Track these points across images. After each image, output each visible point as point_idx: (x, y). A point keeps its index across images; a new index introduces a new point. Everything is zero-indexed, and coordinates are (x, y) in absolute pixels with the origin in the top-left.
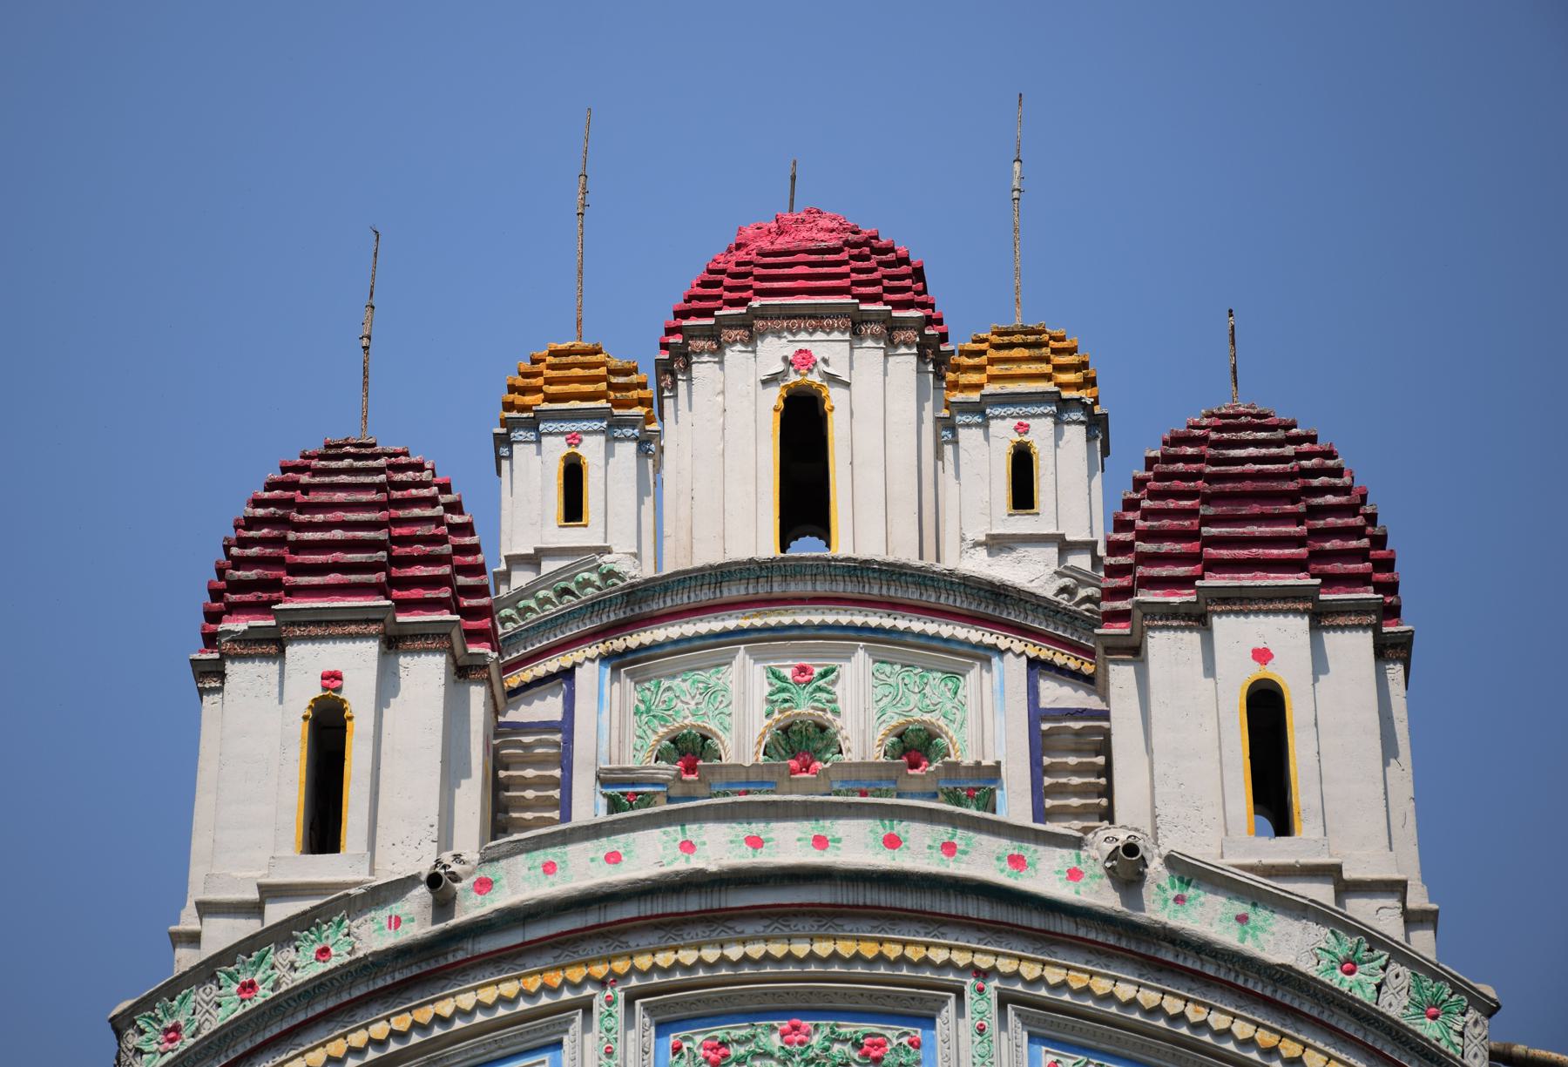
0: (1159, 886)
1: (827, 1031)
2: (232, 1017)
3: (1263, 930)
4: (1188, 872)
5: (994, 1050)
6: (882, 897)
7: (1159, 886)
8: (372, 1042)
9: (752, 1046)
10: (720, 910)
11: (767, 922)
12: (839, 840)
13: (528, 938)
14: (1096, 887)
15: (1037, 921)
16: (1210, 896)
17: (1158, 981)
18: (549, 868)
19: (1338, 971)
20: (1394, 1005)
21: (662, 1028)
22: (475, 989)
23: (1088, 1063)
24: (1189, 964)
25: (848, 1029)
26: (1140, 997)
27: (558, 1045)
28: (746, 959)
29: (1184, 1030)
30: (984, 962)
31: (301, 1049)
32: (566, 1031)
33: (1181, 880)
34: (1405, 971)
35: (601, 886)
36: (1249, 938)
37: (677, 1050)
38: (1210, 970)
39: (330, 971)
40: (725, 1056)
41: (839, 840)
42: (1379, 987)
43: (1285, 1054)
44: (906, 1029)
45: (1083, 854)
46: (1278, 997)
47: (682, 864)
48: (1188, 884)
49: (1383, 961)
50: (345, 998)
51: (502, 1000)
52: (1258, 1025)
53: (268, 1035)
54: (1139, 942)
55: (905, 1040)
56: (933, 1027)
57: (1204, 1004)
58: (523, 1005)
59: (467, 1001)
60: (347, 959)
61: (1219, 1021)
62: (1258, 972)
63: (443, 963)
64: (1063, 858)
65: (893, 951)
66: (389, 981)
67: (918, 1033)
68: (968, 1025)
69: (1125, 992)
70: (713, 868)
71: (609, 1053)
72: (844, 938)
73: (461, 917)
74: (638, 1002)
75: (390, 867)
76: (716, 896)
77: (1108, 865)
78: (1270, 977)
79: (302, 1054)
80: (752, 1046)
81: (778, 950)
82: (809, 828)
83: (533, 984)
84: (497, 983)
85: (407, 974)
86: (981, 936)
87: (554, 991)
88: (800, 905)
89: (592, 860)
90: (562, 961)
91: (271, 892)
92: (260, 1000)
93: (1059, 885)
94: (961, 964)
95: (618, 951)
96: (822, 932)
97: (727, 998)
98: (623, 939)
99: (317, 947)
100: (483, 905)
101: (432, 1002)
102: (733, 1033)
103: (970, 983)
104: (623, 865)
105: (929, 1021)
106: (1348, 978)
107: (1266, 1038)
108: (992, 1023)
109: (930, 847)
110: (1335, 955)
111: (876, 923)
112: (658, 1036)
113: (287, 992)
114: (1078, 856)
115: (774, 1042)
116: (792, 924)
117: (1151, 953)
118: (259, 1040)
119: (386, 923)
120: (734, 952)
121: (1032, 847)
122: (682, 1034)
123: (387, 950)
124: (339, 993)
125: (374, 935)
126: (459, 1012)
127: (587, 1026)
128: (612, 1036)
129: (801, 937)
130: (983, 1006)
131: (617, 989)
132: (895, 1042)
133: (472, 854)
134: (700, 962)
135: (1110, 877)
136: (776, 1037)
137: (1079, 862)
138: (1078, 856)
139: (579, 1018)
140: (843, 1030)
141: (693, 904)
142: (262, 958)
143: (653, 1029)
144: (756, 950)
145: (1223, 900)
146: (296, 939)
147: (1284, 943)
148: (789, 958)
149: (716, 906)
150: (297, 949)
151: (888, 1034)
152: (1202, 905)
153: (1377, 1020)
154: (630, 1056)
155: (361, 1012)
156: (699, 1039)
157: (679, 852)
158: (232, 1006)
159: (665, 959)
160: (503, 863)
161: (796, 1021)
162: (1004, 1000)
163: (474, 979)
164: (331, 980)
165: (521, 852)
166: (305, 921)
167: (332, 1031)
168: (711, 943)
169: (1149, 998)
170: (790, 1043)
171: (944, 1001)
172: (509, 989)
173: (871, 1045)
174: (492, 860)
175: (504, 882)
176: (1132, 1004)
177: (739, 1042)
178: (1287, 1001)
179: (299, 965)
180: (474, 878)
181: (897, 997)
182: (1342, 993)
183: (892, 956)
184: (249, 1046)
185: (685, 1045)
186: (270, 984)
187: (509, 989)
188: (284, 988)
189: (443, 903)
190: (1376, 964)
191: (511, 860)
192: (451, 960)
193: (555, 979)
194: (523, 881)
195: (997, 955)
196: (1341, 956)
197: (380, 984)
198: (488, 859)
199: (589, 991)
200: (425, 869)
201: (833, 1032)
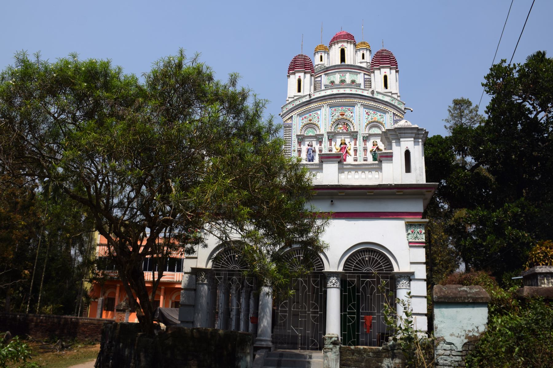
4: (378, 93)
20: (396, 104)
64: (367, 92)
82: (343, 89)
91: (295, 96)
125: (304, 100)
141: (333, 97)
147: (387, 99)
166: (298, 99)
179: (298, 103)
189: (310, 97)
194: (317, 95)
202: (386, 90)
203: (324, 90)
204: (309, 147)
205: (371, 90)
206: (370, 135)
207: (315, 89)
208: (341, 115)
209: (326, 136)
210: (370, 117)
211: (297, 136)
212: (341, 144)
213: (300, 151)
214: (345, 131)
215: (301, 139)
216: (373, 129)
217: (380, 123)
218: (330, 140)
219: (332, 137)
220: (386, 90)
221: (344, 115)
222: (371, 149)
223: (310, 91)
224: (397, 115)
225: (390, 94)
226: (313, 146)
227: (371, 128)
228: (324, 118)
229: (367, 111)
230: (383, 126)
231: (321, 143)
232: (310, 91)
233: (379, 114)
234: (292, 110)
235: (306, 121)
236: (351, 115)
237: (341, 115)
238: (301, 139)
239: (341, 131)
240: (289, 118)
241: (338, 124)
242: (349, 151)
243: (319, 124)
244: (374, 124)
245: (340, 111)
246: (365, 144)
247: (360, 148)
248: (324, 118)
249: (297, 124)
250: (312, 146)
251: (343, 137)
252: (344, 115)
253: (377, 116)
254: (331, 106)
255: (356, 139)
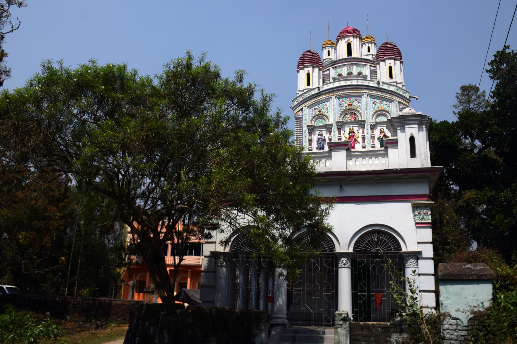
4: (384, 83)
20: (401, 93)
47: (339, 85)
64: (373, 82)
82: (350, 81)
91: (304, 89)
125: (313, 92)
147: (392, 88)
179: (307, 95)
189: (319, 89)
194: (326, 87)
202: (392, 81)
203: (332, 83)
204: (319, 137)
205: (376, 81)
206: (378, 123)
207: (324, 82)
208: (349, 105)
209: (335, 126)
210: (377, 106)
211: (308, 126)
212: (350, 133)
213: (310, 141)
214: (353, 120)
215: (311, 129)
216: (380, 117)
217: (386, 111)
218: (339, 129)
219: (340, 126)
220: (392, 81)
221: (351, 105)
222: (378, 136)
223: (319, 84)
224: (402, 103)
225: (395, 84)
226: (323, 135)
227: (378, 116)
228: (333, 110)
229: (373, 100)
230: (390, 114)
231: (330, 132)
232: (319, 84)
233: (385, 103)
234: (302, 103)
235: (315, 112)
236: (359, 105)
237: (349, 105)
238: (311, 129)
239: (349, 121)
240: (299, 110)
241: (346, 114)
242: (357, 139)
243: (328, 114)
244: (380, 113)
245: (347, 102)
246: (373, 132)
247: (368, 136)
248: (333, 110)
249: (308, 115)
250: (322, 135)
251: (351, 126)
252: (351, 105)
253: (384, 105)
254: (339, 97)
255: (364, 127)
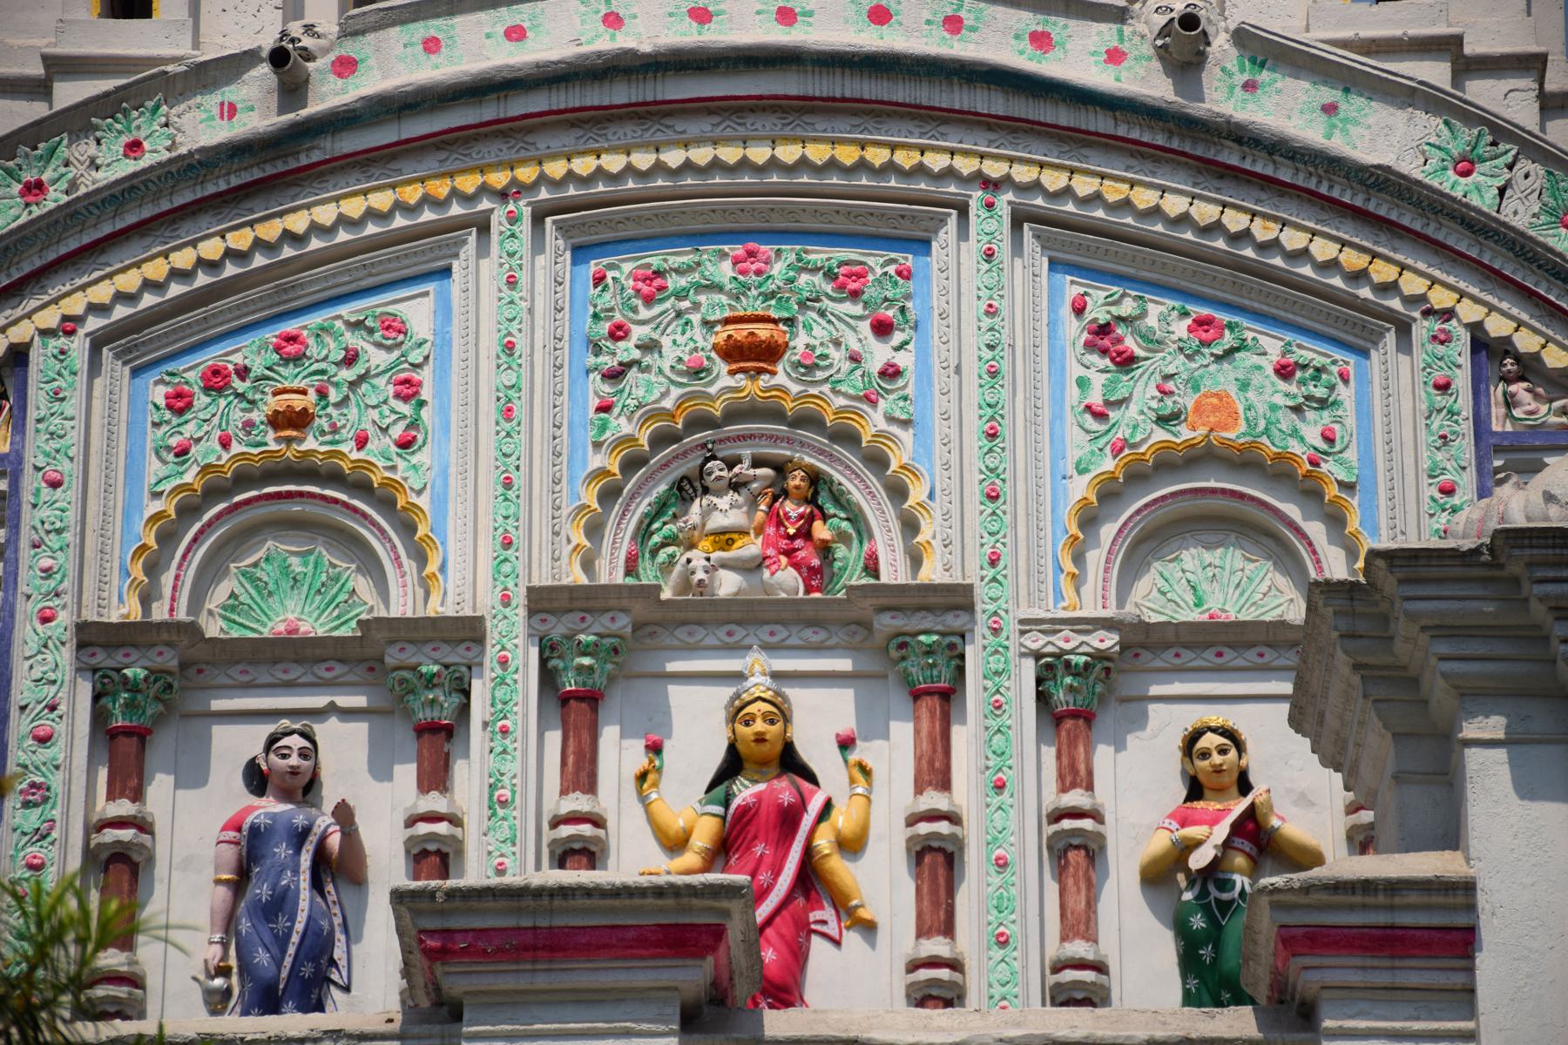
0: (1223, 70)
1: (792, 257)
2: (14, 225)
3: (1356, 122)
4: (1264, 51)
5: (1004, 280)
6: (866, 87)
7: (1223, 70)
8: (201, 263)
9: (696, 277)
10: (656, 103)
11: (716, 119)
12: (810, 14)
13: (404, 136)
14: (1142, 72)
15: (1063, 116)
16: (1289, 80)
17: (1218, 190)
18: (432, 45)
19: (1450, 172)
20: (1521, 214)
21: (580, 253)
22: (337, 199)
23: (1124, 295)
24: (1258, 169)
25: (819, 255)
26: (1193, 211)
27: (446, 272)
28: (688, 166)
29: (1249, 252)
30: (995, 169)
31: (108, 270)
32: (457, 256)
33: (1253, 61)
34: (1537, 169)
35: (500, 69)
36: (1337, 132)
37: (599, 280)
38: (1285, 175)
39: (144, 171)
40: (662, 288)
41: (810, 14)
42: (1502, 191)
43: (1376, 278)
44: (893, 255)
45: (1127, 30)
46: (1371, 207)
48: (1262, 65)
49: (1509, 158)
50: (165, 206)
51: (372, 214)
52: (1344, 243)
53: (63, 250)
54: (1195, 140)
55: (891, 269)
56: (928, 253)
57: (1275, 219)
58: (399, 222)
59: (326, 214)
60: (166, 156)
61: (1293, 240)
62: (1347, 177)
63: (293, 165)
64: (1101, 34)
65: (878, 156)
66: (223, 186)
67: (909, 260)
68: (972, 249)
69: (1175, 205)
70: (646, 48)
71: (512, 282)
72: (815, 140)
73: (314, 107)
74: (549, 220)
75: (220, 40)
76: (650, 85)
77: (1159, 43)
78: (1362, 182)
79: (110, 276)
80: (696, 277)
81: (730, 154)
83: (412, 194)
84: (365, 193)
85: (246, 177)
86: (992, 136)
87: (439, 204)
88: (760, 97)
89: (488, 36)
90: (448, 167)
91: (62, 66)
92: (51, 205)
93: (1094, 70)
94: (965, 172)
95: (523, 154)
96: (787, 131)
97: (665, 215)
98: (529, 138)
99: (125, 139)
100: (344, 91)
101: (281, 214)
102: (671, 259)
103: (976, 196)
104: (528, 43)
105: (923, 245)
106: (1463, 180)
107: (1352, 260)
108: (1004, 248)
109: (928, 22)
110: (1447, 152)
111: (856, 121)
112: (574, 263)
113: (87, 195)
114: (1121, 32)
115: (724, 271)
116: (749, 122)
117: (1210, 155)
118: (51, 256)
119: (216, 111)
120: (674, 158)
121: (1062, 21)
122: (606, 261)
123: (220, 145)
124: (156, 198)
125: (201, 126)
126: (316, 228)
127: (483, 251)
128: (515, 262)
129: (760, 139)
130: (991, 226)
131: (522, 203)
132: (879, 271)
133: (329, 24)
134: (630, 170)
135: (1161, 58)
136: (727, 266)
137: (1121, 40)
138: (1121, 32)
139: (472, 239)
140: (812, 257)
142: (53, 151)
143: (568, 255)
144: (702, 155)
145: (1306, 85)
146: (97, 128)
148: (744, 164)
149: (650, 98)
150: (98, 142)
151: (871, 261)
152: (1279, 92)
153: (1497, 233)
154: (539, 288)
155: (187, 225)
156: (628, 267)
157: (602, 28)
158: (13, 212)
159: (584, 165)
160: (370, 37)
161: (752, 245)
162: (1019, 219)
163: (335, 187)
164: (145, 183)
165: (393, 24)
166: (108, 105)
167: (149, 247)
168: (643, 146)
169: (1205, 212)
170: (743, 272)
171: (943, 221)
172: (382, 200)
173: (848, 276)
174: (355, 34)
175: (372, 62)
176: (1184, 220)
177: (677, 271)
178: (1382, 212)
179: (104, 162)
180: (332, 57)
181: (882, 215)
182: (1454, 199)
183: (877, 163)
184: (38, 263)
185: (610, 274)
186: (63, 185)
187: (382, 200)
188: (82, 190)
189: (292, 89)
190: (1500, 162)
191: (381, 34)
192: (304, 161)
193: (441, 188)
195: (1011, 160)
196: (1455, 153)
197: (211, 189)
198: (350, 31)
199: (485, 204)
200: (268, 42)
201: (799, 260)
